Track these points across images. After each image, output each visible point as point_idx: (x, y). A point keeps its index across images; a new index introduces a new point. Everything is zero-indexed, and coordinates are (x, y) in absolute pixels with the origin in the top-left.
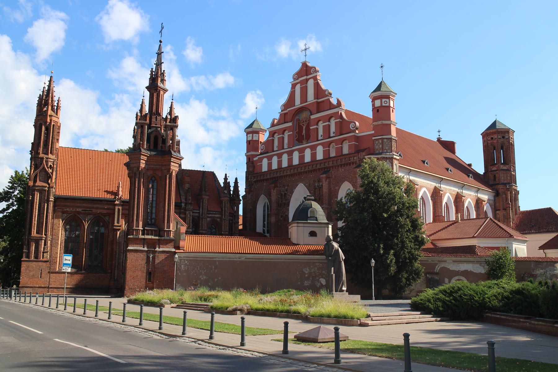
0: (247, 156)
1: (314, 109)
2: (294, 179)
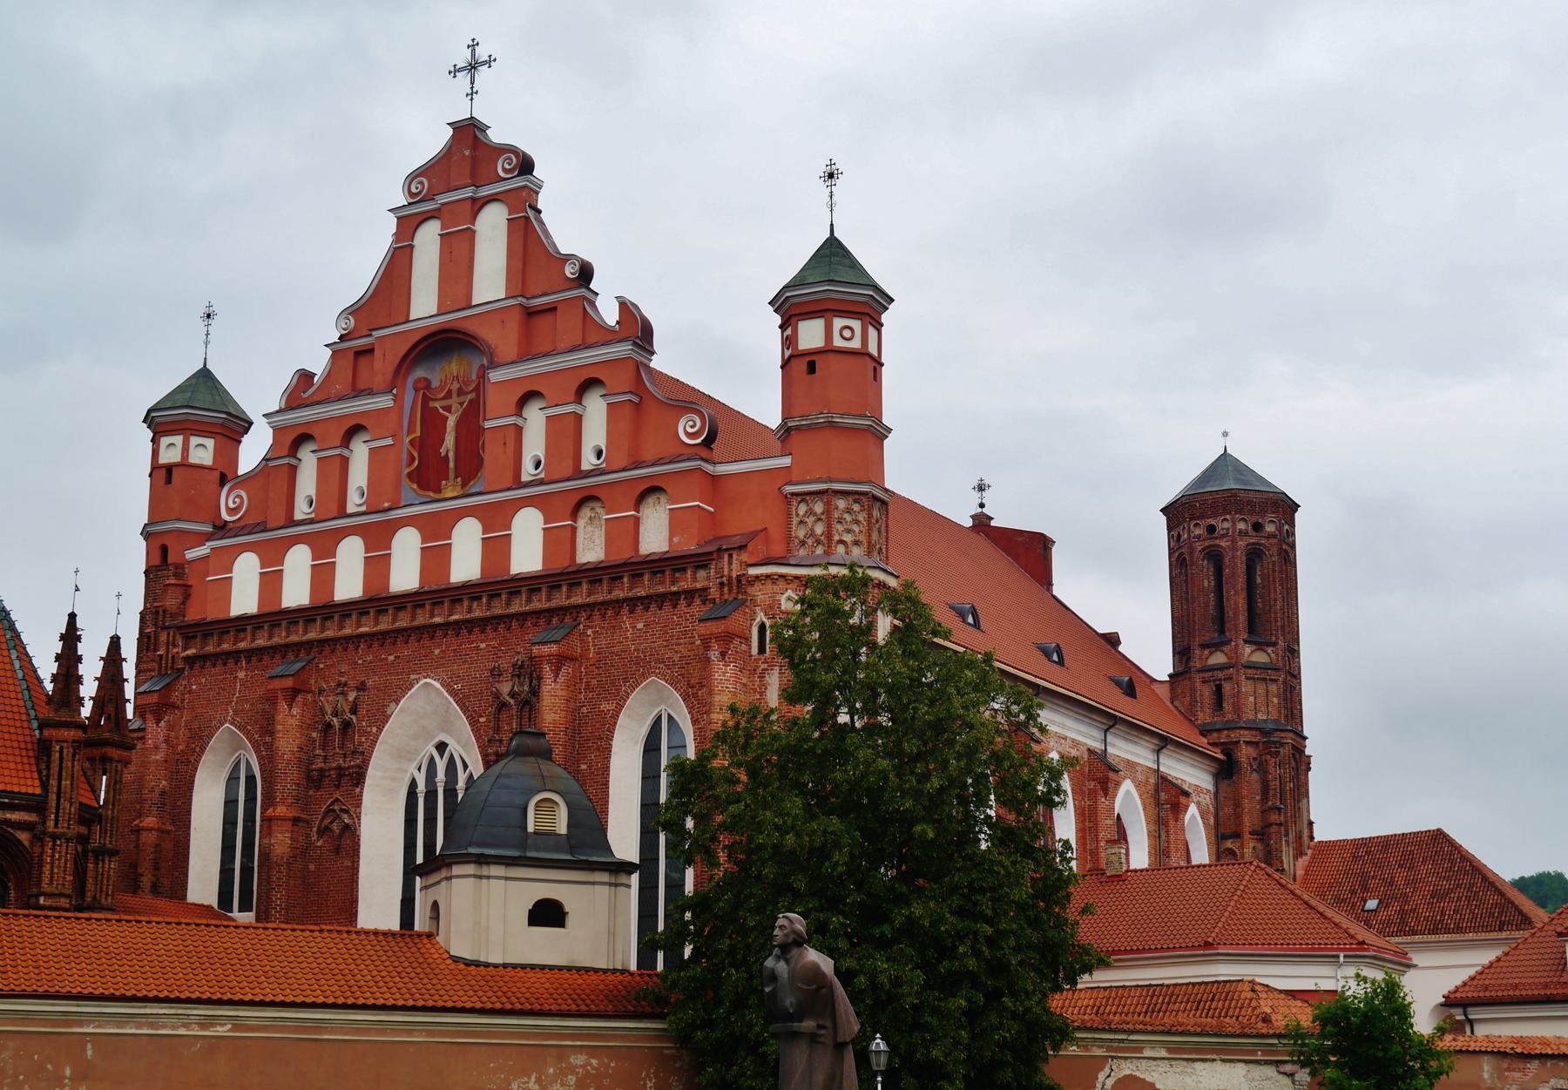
0: (147, 534)
1: (503, 339)
2: (391, 658)
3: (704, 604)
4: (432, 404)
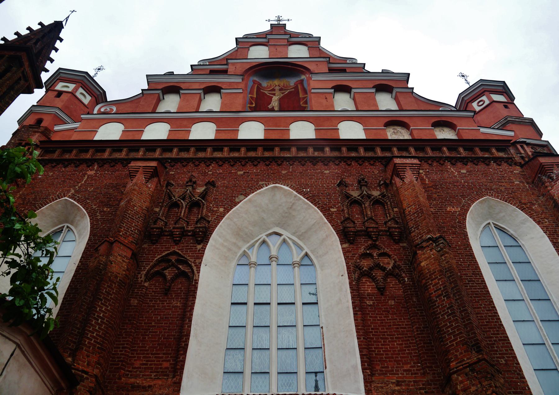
3: (510, 165)
4: (261, 90)
